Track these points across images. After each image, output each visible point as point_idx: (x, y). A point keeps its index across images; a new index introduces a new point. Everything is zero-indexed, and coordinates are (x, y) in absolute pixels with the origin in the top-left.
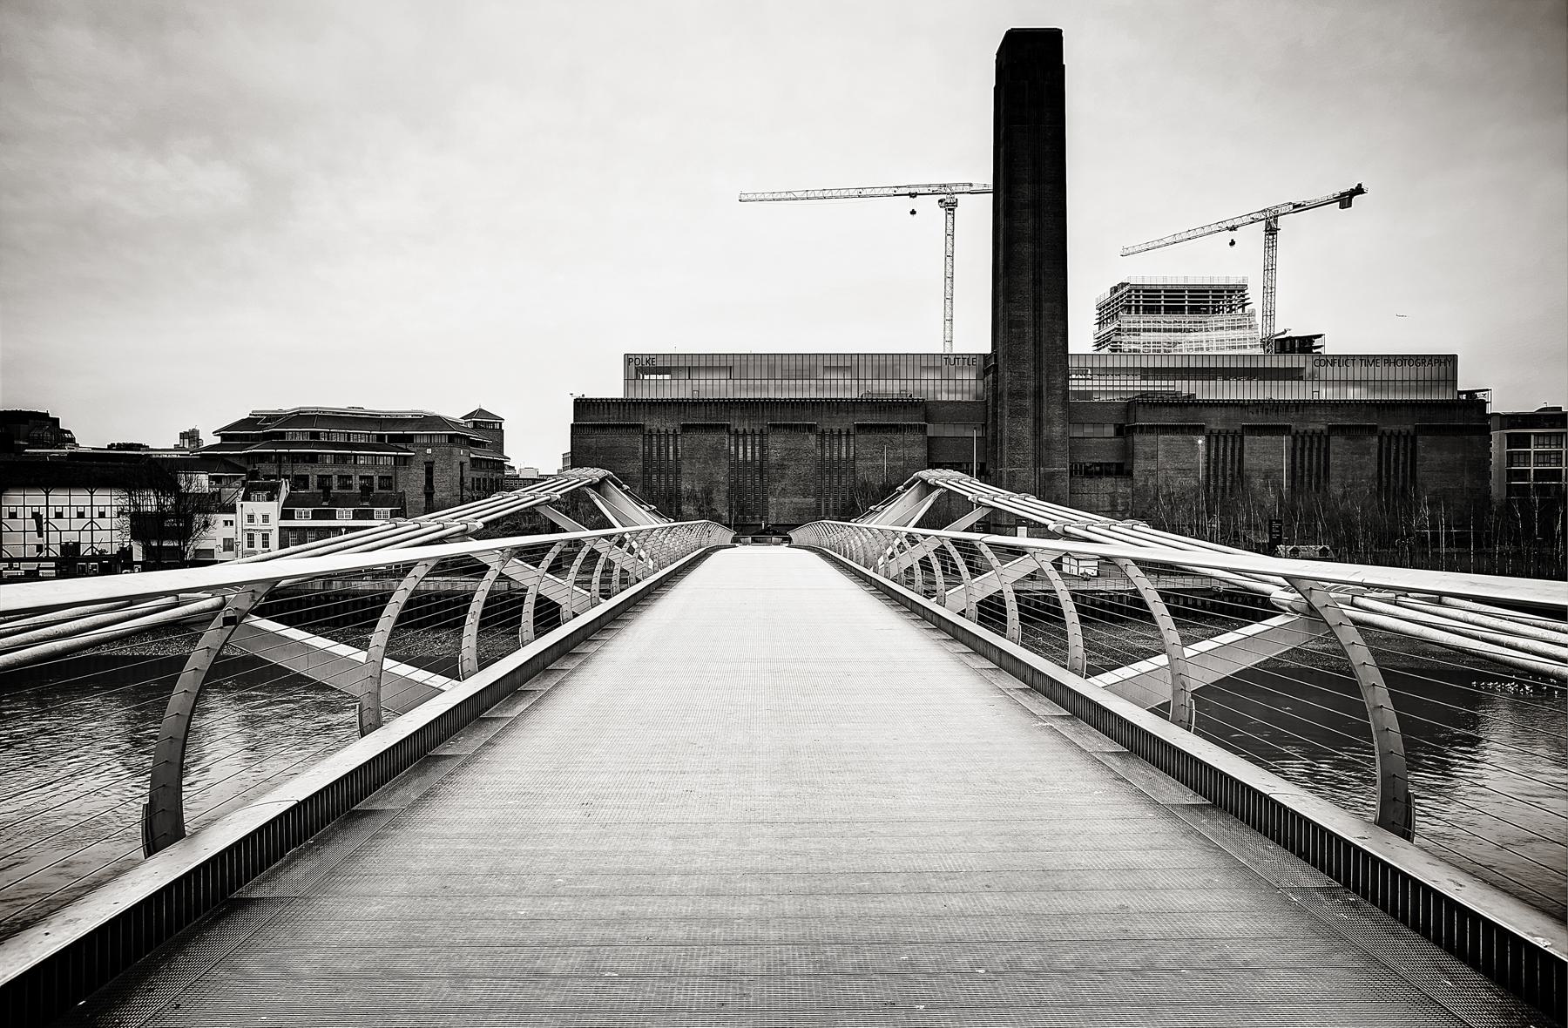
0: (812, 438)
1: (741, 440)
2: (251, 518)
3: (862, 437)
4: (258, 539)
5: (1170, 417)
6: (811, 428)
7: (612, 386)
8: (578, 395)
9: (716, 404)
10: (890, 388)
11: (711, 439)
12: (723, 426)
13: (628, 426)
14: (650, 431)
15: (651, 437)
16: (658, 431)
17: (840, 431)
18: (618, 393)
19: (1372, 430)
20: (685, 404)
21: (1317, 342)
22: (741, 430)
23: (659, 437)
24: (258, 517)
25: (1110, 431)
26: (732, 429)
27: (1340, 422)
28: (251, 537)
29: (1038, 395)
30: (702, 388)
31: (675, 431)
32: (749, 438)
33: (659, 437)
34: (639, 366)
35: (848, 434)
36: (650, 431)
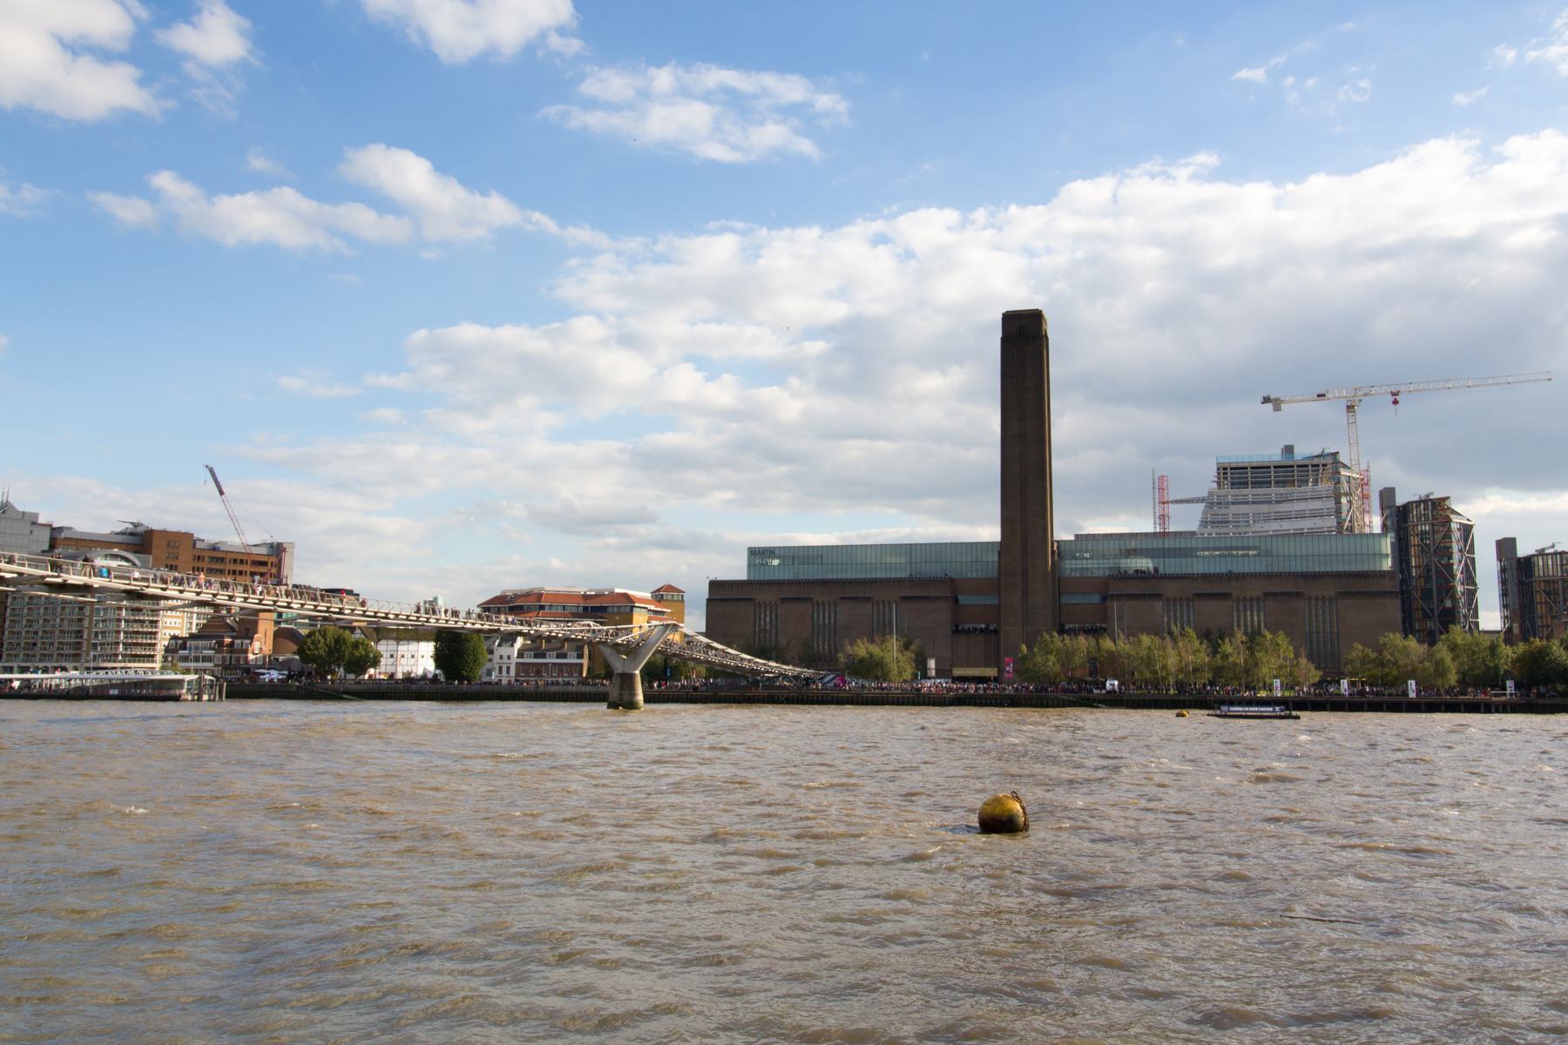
0: (870, 606)
2: (501, 657)
4: (504, 669)
5: (1135, 588)
6: (868, 599)
7: (736, 569)
8: (712, 578)
10: (935, 570)
12: (808, 599)
15: (760, 607)
18: (742, 575)
19: (1298, 595)
21: (1447, 503)
23: (766, 607)
24: (505, 657)
25: (1096, 599)
26: (815, 600)
27: (1273, 589)
28: (501, 668)
29: (1025, 573)
30: (801, 571)
32: (827, 607)
33: (766, 607)
34: (758, 555)
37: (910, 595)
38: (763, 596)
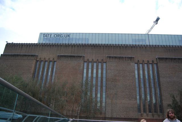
0: (132, 64)
1: (90, 65)
3: (161, 65)
8: (10, 42)
9: (78, 46)
11: (73, 63)
13: (29, 55)
14: (40, 59)
16: (45, 59)
17: (148, 61)
20: (61, 46)
22: (90, 60)
26: (86, 59)
31: (54, 59)
35: (153, 61)
36: (40, 59)
37: (164, 57)
38: (43, 55)
